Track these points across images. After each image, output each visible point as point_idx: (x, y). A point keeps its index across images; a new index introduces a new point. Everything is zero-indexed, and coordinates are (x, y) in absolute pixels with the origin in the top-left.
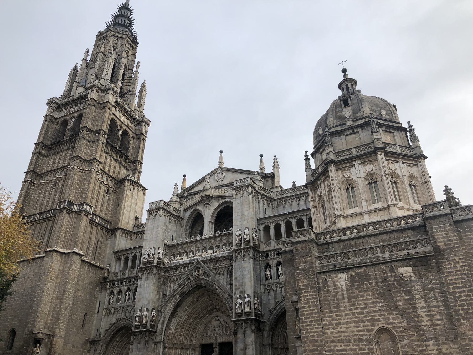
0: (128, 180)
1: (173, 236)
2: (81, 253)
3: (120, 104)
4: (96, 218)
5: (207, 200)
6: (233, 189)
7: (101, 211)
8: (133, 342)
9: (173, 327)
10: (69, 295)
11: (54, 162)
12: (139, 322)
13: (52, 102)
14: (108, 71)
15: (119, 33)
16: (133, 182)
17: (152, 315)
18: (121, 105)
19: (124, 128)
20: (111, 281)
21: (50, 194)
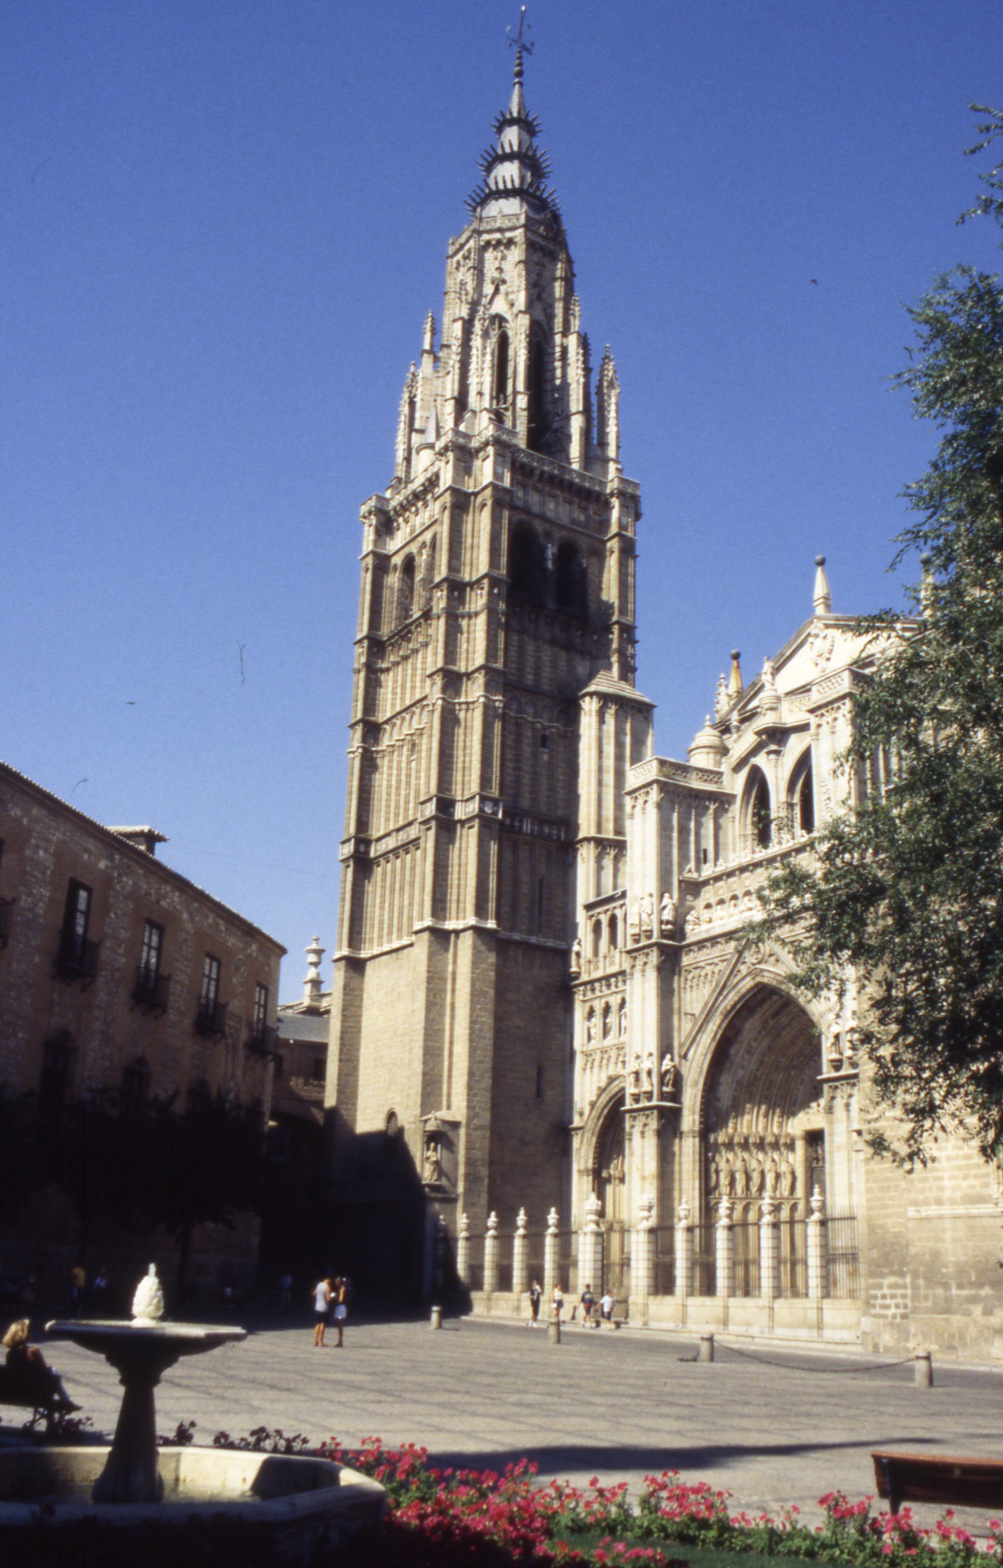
0: (591, 695)
1: (705, 851)
2: (491, 924)
3: (532, 470)
4: (521, 822)
5: (776, 736)
6: (812, 711)
7: (534, 800)
8: (631, 1134)
9: (725, 1094)
10: (481, 1030)
11: (403, 687)
12: (636, 1086)
13: (370, 513)
14: (482, 378)
15: (500, 230)
16: (606, 699)
17: (664, 1068)
18: (537, 472)
19: (558, 534)
20: (585, 984)
21: (408, 776)
